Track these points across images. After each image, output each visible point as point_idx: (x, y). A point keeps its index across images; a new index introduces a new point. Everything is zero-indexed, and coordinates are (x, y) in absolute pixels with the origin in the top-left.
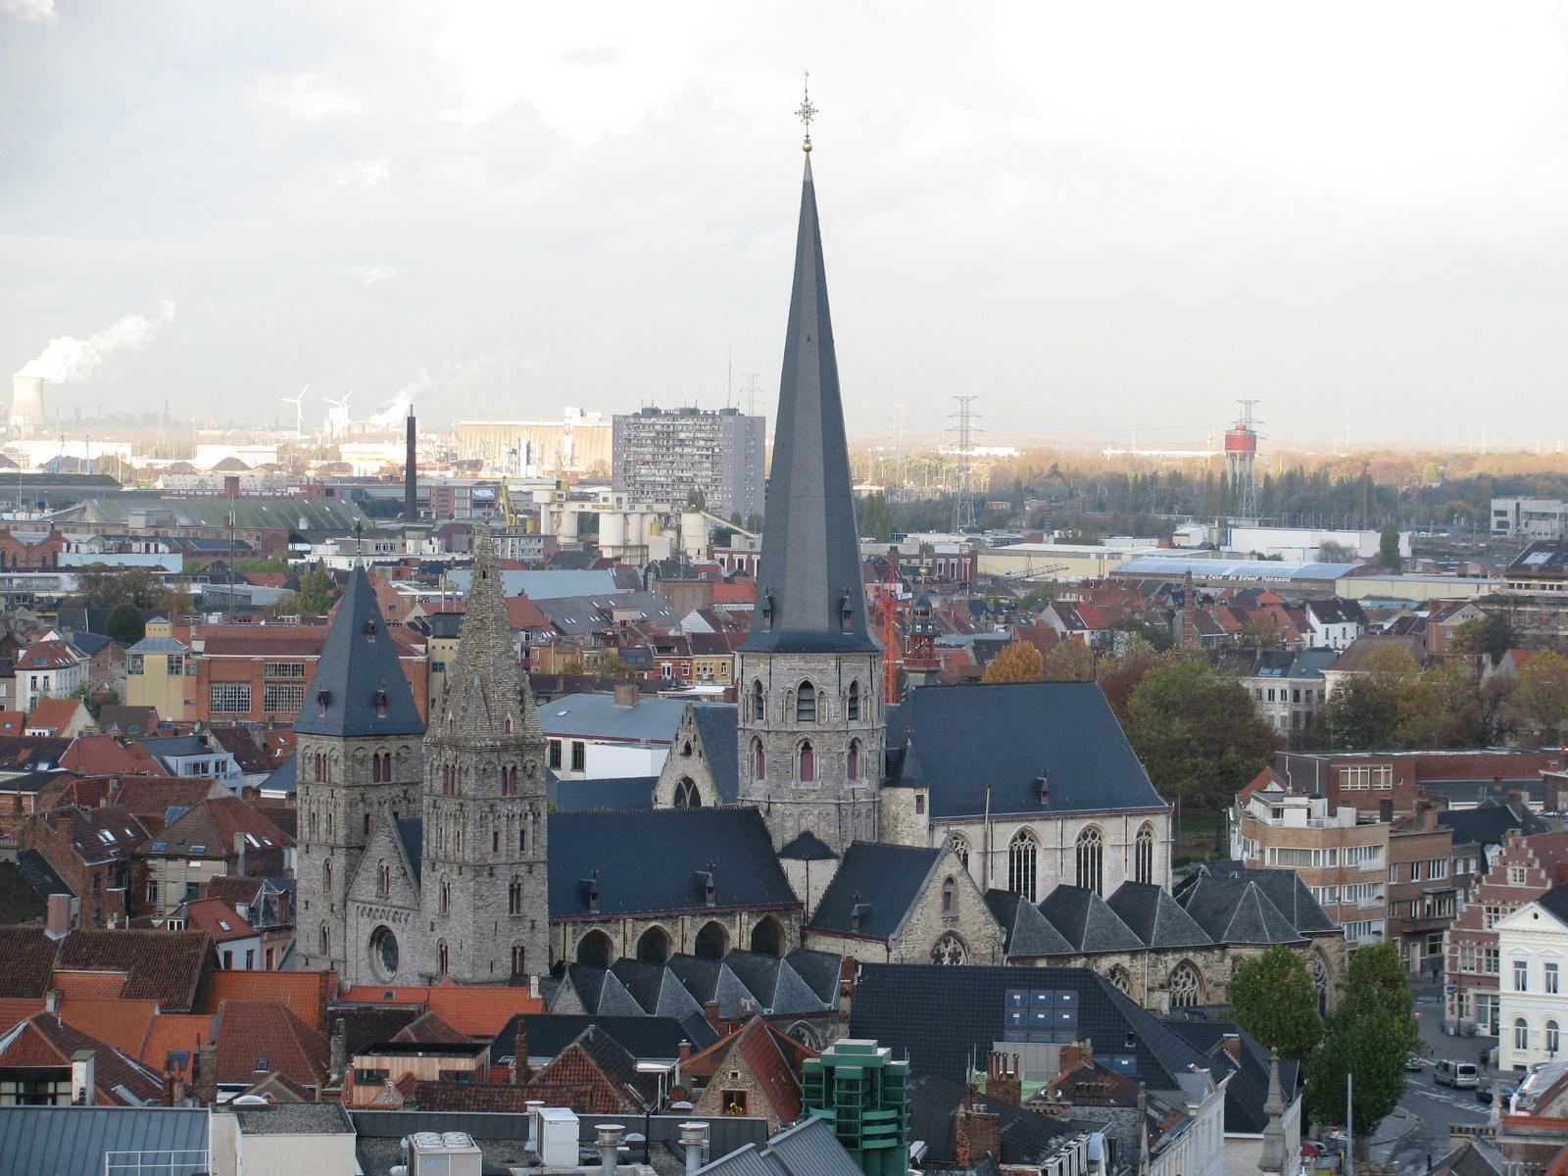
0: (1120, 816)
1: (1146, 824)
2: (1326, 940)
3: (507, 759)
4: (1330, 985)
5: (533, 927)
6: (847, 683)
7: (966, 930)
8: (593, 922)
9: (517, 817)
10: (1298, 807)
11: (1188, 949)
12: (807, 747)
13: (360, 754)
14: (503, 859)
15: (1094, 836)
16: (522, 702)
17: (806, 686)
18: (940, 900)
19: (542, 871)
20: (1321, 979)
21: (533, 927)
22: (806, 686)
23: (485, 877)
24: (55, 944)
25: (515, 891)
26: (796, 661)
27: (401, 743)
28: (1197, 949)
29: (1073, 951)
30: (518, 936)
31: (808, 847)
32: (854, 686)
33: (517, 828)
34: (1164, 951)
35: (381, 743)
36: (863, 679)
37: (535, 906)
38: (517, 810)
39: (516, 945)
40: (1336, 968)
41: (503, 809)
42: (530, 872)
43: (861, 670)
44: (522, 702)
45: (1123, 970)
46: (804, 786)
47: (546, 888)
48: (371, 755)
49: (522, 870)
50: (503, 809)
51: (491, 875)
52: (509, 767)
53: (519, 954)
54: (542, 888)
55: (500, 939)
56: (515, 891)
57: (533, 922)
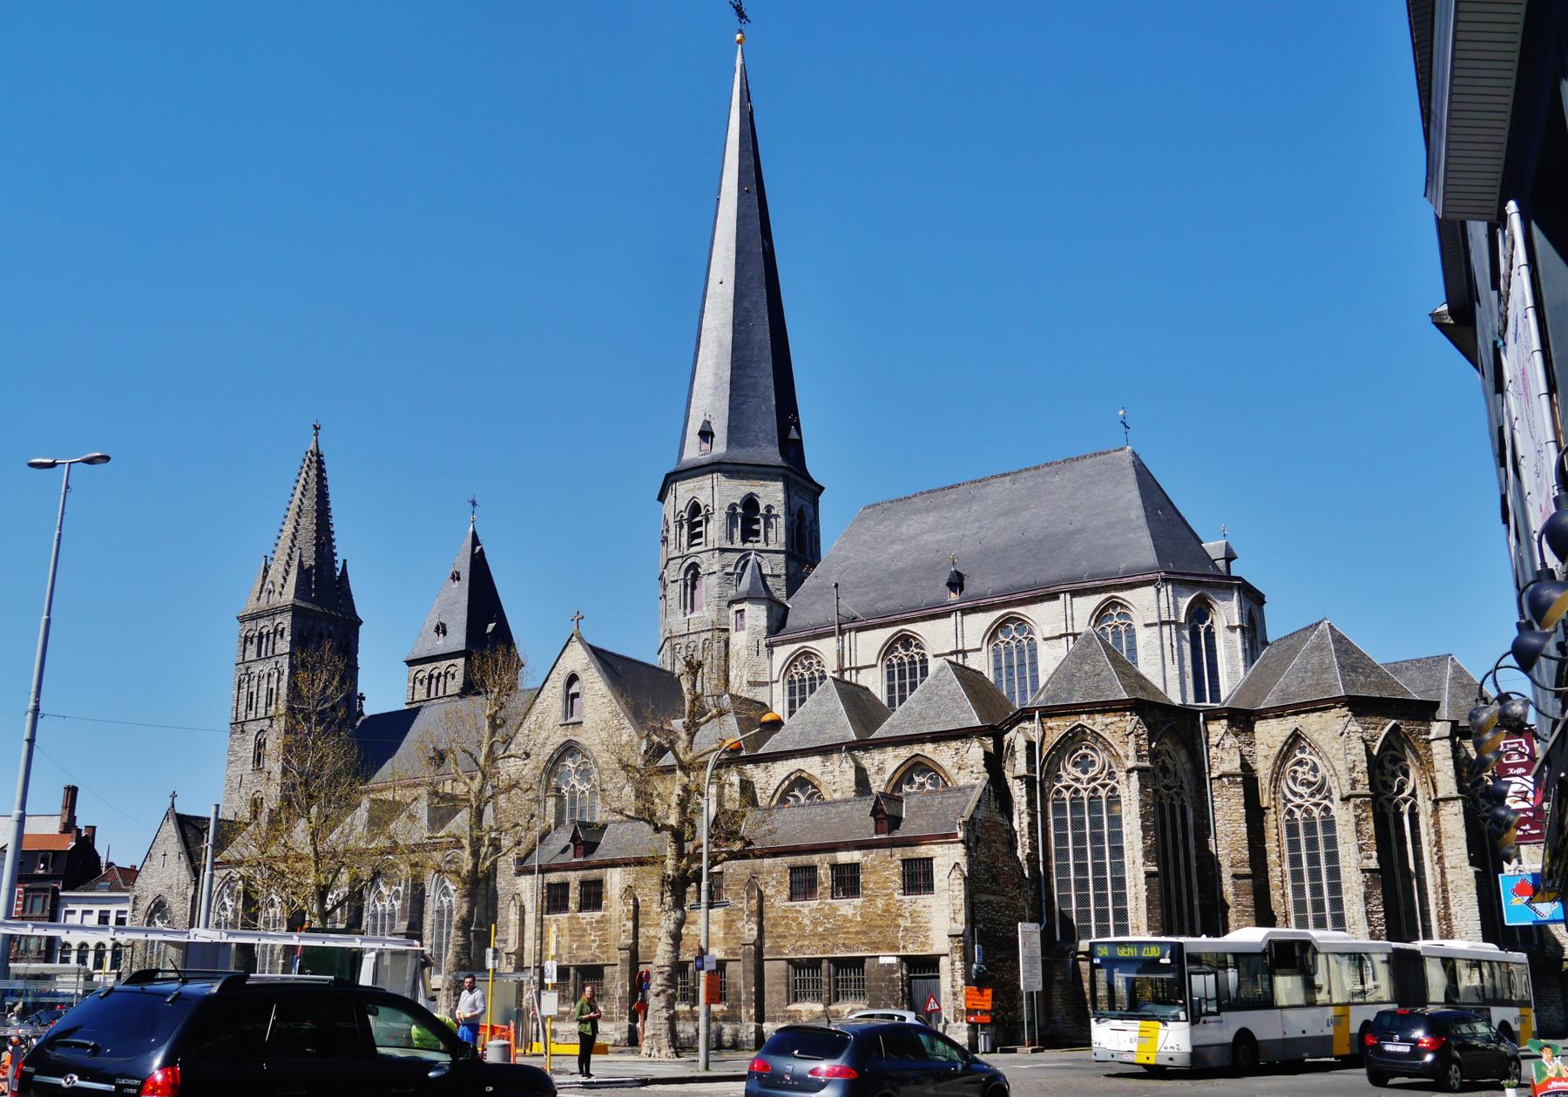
0: (1054, 596)
2: (1314, 717)
4: (1336, 796)
6: (682, 505)
11: (920, 739)
13: (420, 676)
20: (1319, 790)
25: (260, 745)
27: (449, 662)
28: (938, 738)
32: (695, 509)
36: (703, 500)
38: (266, 671)
40: (1341, 767)
41: (256, 669)
43: (701, 488)
50: (256, 669)
52: (265, 631)
55: (243, 792)
56: (260, 745)
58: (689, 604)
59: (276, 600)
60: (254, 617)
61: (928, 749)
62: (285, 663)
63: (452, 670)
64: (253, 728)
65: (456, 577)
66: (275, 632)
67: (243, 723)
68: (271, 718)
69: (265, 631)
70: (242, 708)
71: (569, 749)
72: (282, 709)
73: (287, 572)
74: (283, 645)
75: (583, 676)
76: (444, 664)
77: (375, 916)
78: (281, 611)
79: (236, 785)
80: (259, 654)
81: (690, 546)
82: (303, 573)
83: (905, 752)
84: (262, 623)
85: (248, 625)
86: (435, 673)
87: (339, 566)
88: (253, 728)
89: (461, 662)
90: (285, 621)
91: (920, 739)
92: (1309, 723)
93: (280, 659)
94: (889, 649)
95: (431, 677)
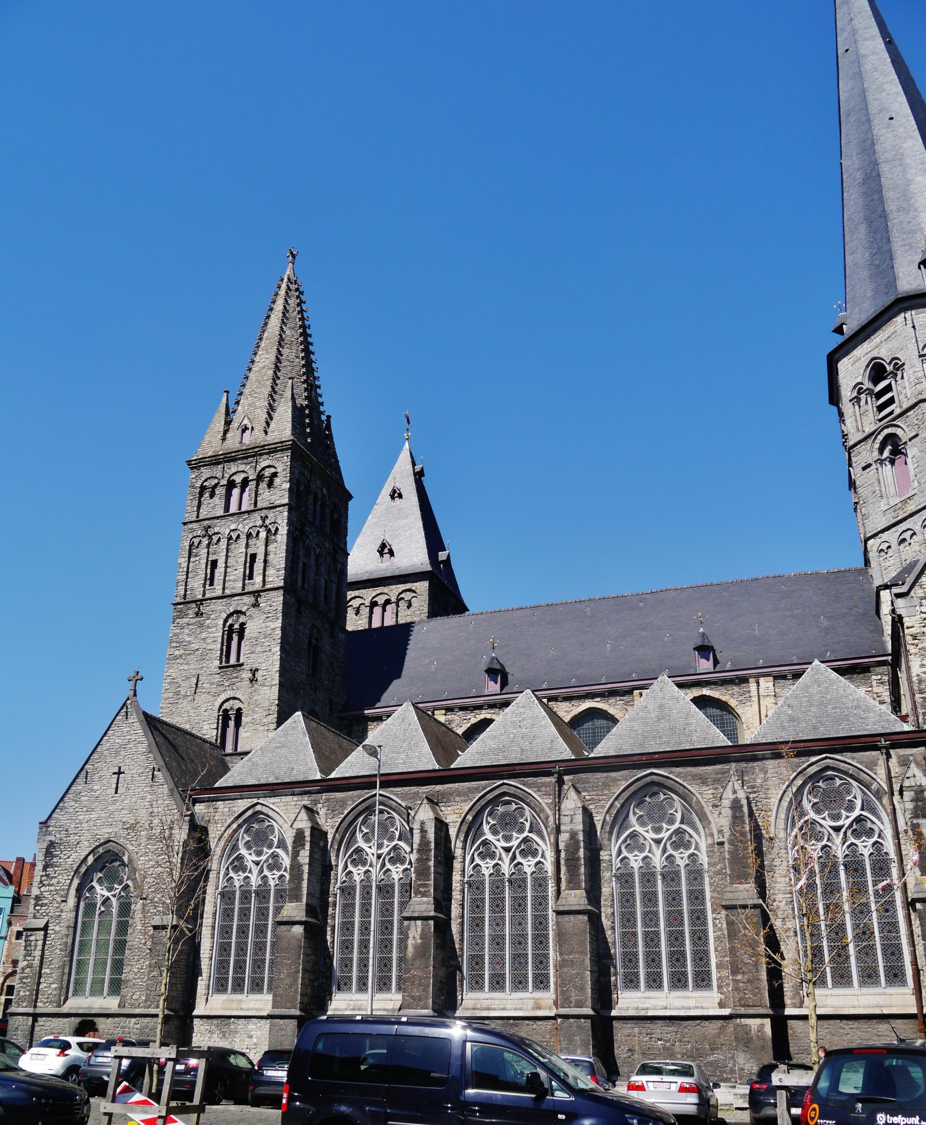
3: (233, 470)
5: (253, 680)
8: (479, 707)
9: (243, 537)
14: (219, 593)
21: (253, 680)
23: (190, 617)
25: (234, 633)
30: (229, 694)
33: (239, 549)
35: (379, 590)
37: (259, 649)
38: (244, 528)
39: (225, 706)
41: (224, 528)
42: (256, 605)
47: (279, 624)
48: (367, 603)
50: (224, 528)
51: (199, 614)
52: (238, 479)
54: (272, 625)
55: (201, 698)
56: (234, 633)
57: (254, 671)
60: (215, 461)
62: (282, 520)
63: (408, 596)
64: (217, 613)
65: (396, 494)
66: (260, 478)
67: (199, 602)
68: (257, 594)
72: (276, 577)
73: (271, 408)
74: (280, 494)
76: (393, 591)
77: (625, 878)
78: (272, 450)
79: (186, 688)
80: (227, 508)
82: (298, 413)
84: (233, 468)
85: (206, 472)
86: (381, 600)
87: (324, 418)
88: (217, 613)
89: (422, 587)
90: (282, 464)
93: (271, 514)
95: (374, 604)
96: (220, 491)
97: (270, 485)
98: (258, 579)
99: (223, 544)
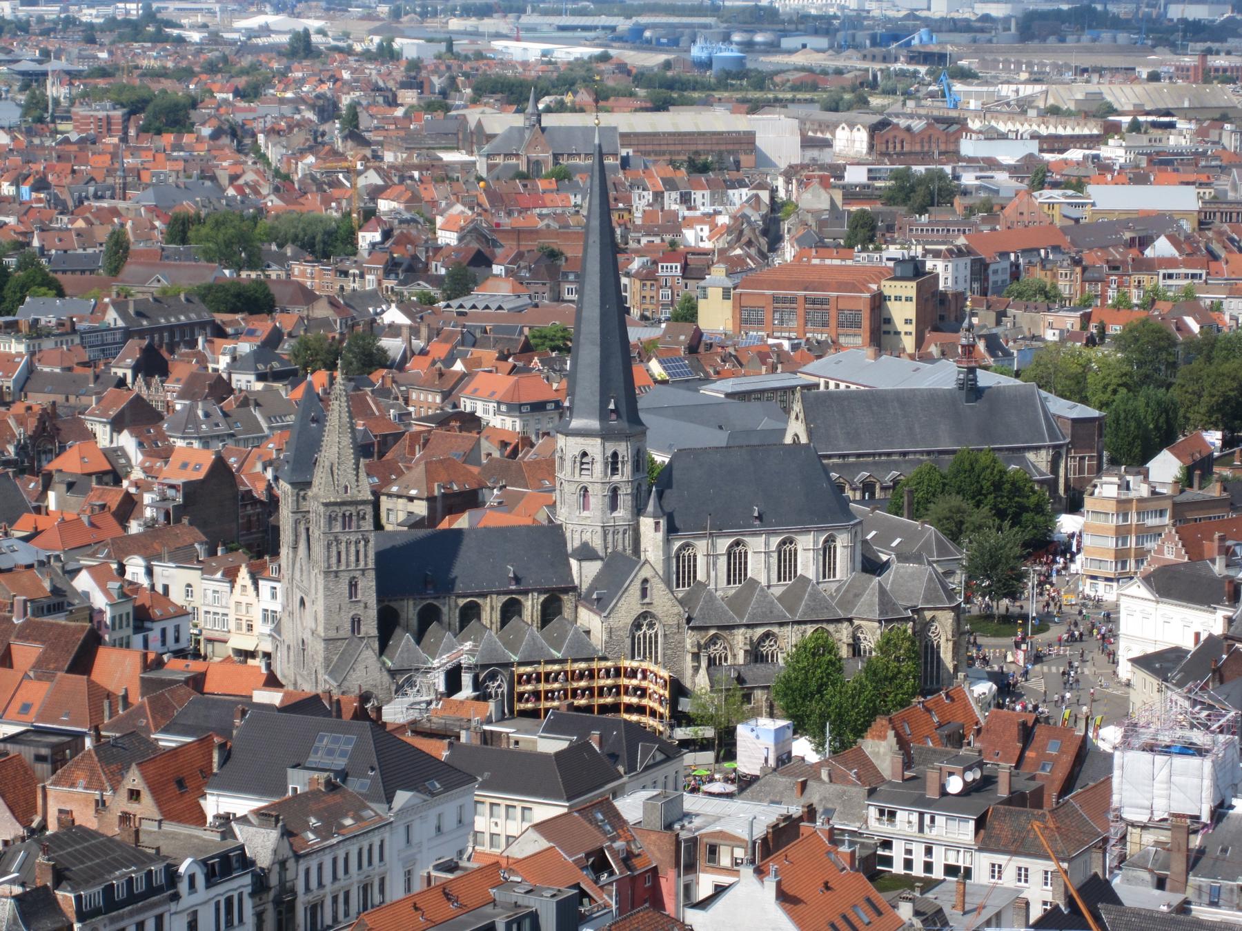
1: (830, 536)
5: (366, 607)
6: (609, 453)
7: (657, 610)
10: (1112, 483)
11: (822, 621)
12: (586, 490)
15: (791, 543)
16: (357, 475)
17: (585, 454)
18: (638, 593)
19: (372, 575)
21: (366, 607)
22: (585, 454)
24: (15, 625)
25: (353, 585)
26: (579, 440)
29: (738, 622)
31: (586, 554)
32: (615, 455)
33: (353, 549)
34: (805, 622)
38: (353, 538)
41: (343, 538)
44: (357, 475)
45: (773, 634)
46: (586, 514)
49: (357, 574)
52: (347, 514)
53: (356, 623)
55: (343, 614)
56: (353, 585)
58: (614, 506)
59: (352, 494)
61: (824, 626)
67: (336, 572)
68: (363, 570)
69: (347, 514)
70: (334, 560)
71: (645, 615)
72: (371, 565)
75: (652, 580)
78: (364, 502)
81: (613, 474)
83: (816, 626)
84: (345, 508)
85: (331, 508)
91: (822, 621)
92: (938, 613)
94: (731, 546)
96: (340, 519)
97: (364, 518)
98: (362, 563)
99: (344, 544)
